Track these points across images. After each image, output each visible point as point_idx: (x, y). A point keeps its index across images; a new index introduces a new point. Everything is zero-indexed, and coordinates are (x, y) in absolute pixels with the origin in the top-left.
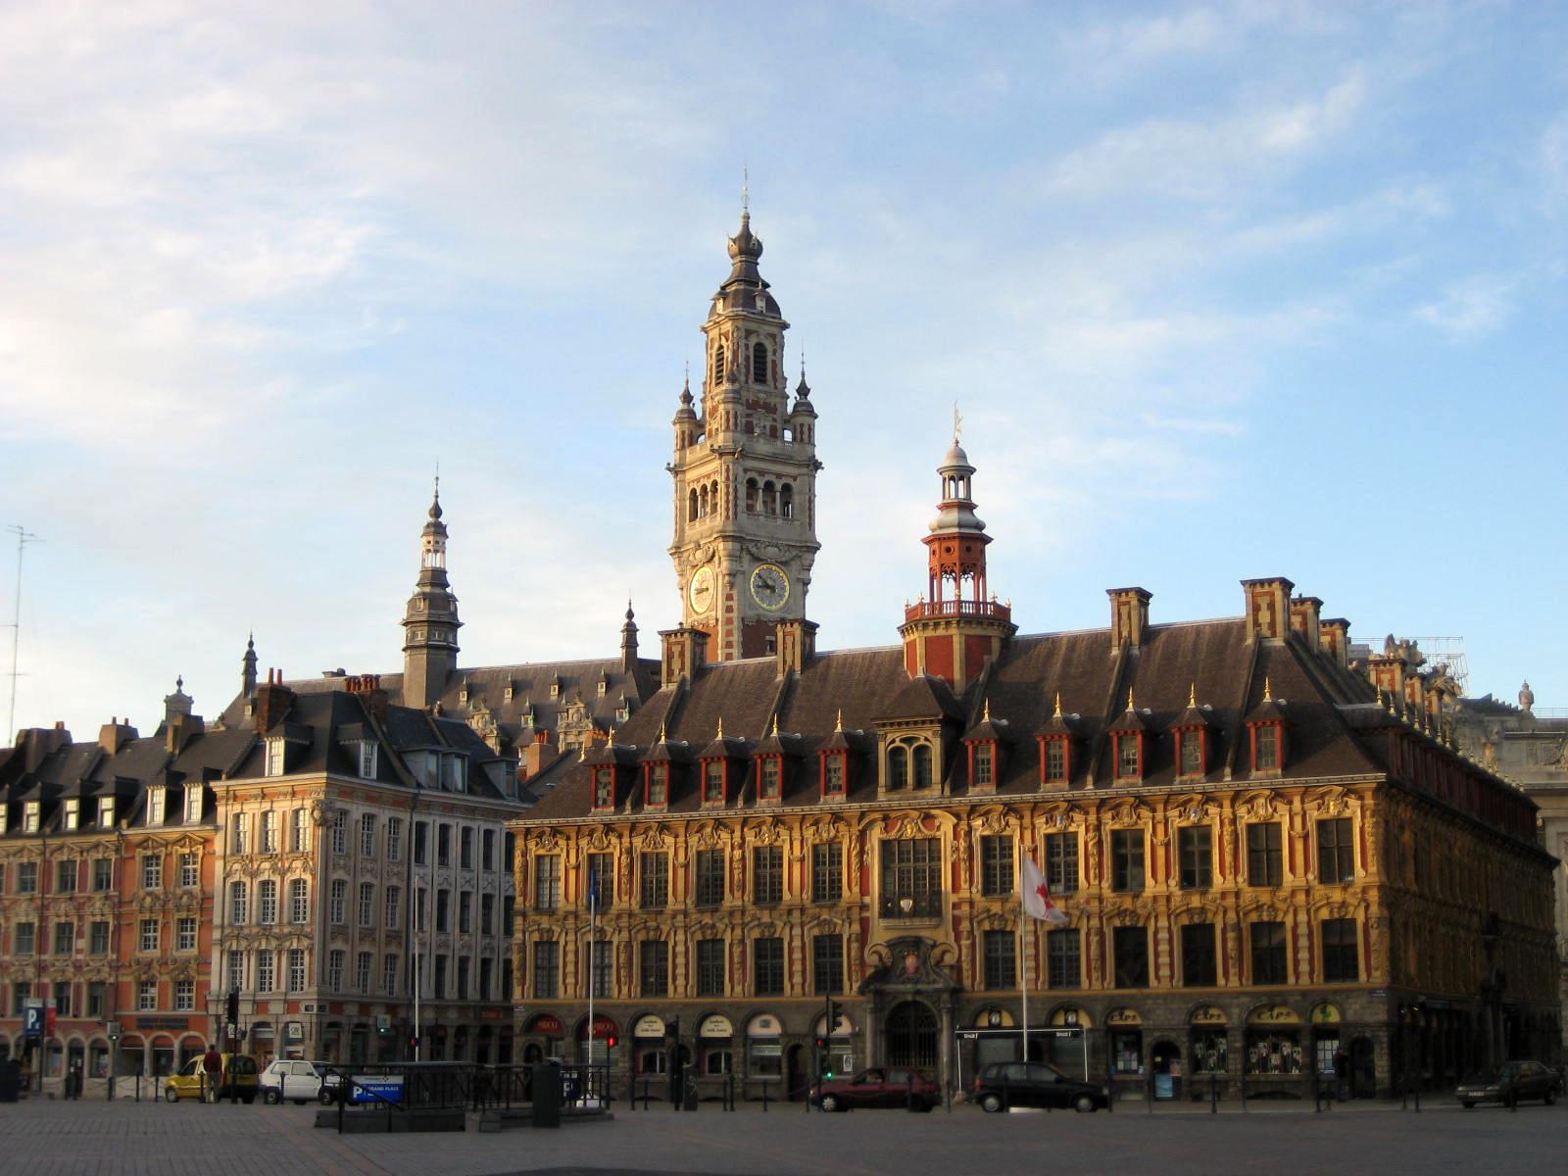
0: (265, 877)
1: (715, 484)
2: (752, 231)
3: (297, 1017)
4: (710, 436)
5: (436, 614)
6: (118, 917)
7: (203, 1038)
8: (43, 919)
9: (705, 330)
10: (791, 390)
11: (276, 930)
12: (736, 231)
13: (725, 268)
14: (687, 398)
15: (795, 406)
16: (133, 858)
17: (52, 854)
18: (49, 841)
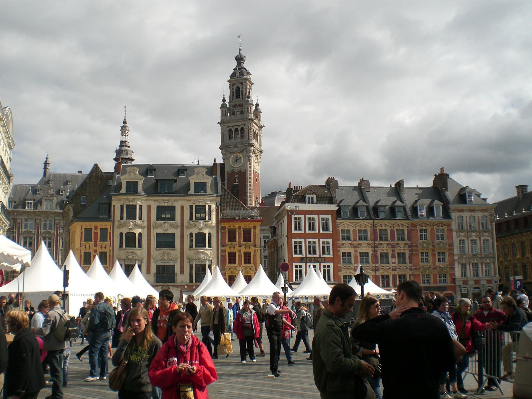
0: (474, 238)
1: (242, 129)
2: (242, 53)
3: (491, 285)
4: (233, 114)
5: (122, 156)
6: (410, 251)
7: (453, 293)
8: (375, 251)
9: (229, 81)
10: (254, 103)
11: (479, 256)
12: (237, 54)
13: (234, 64)
14: (224, 100)
15: (256, 110)
16: (416, 230)
17: (376, 227)
18: (375, 221)
